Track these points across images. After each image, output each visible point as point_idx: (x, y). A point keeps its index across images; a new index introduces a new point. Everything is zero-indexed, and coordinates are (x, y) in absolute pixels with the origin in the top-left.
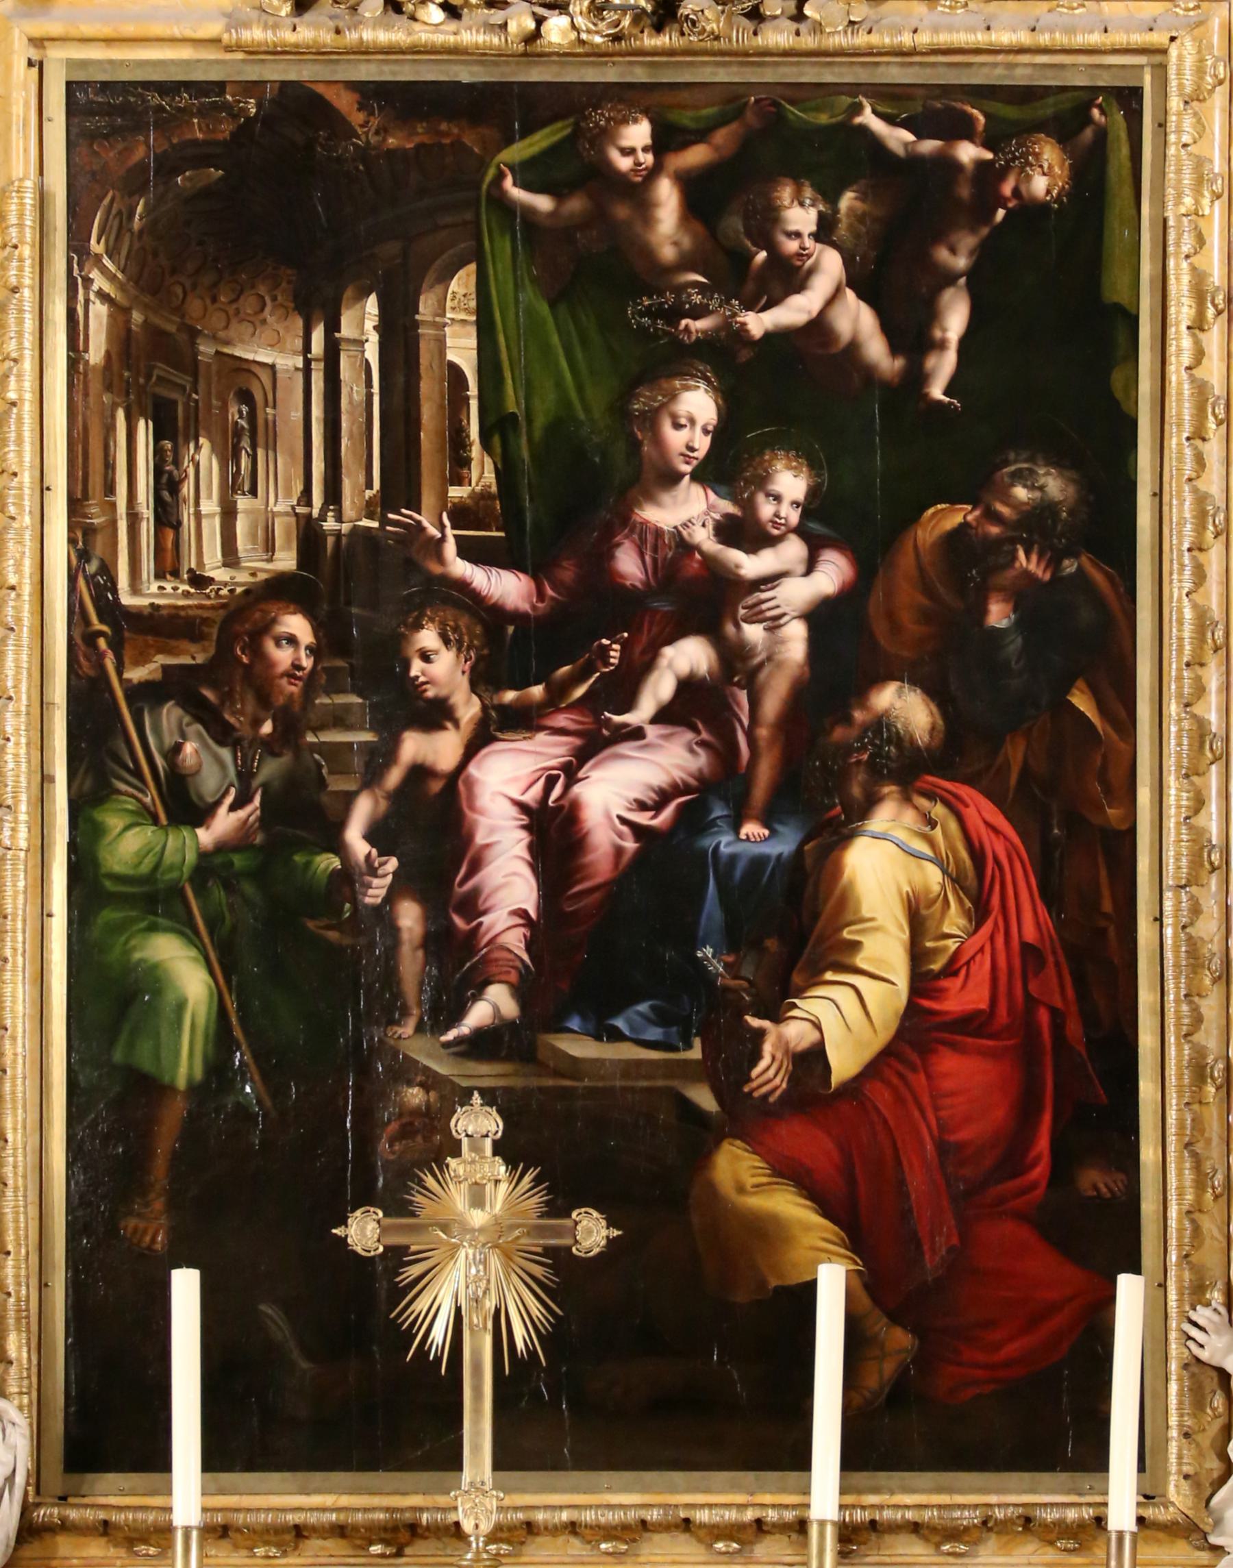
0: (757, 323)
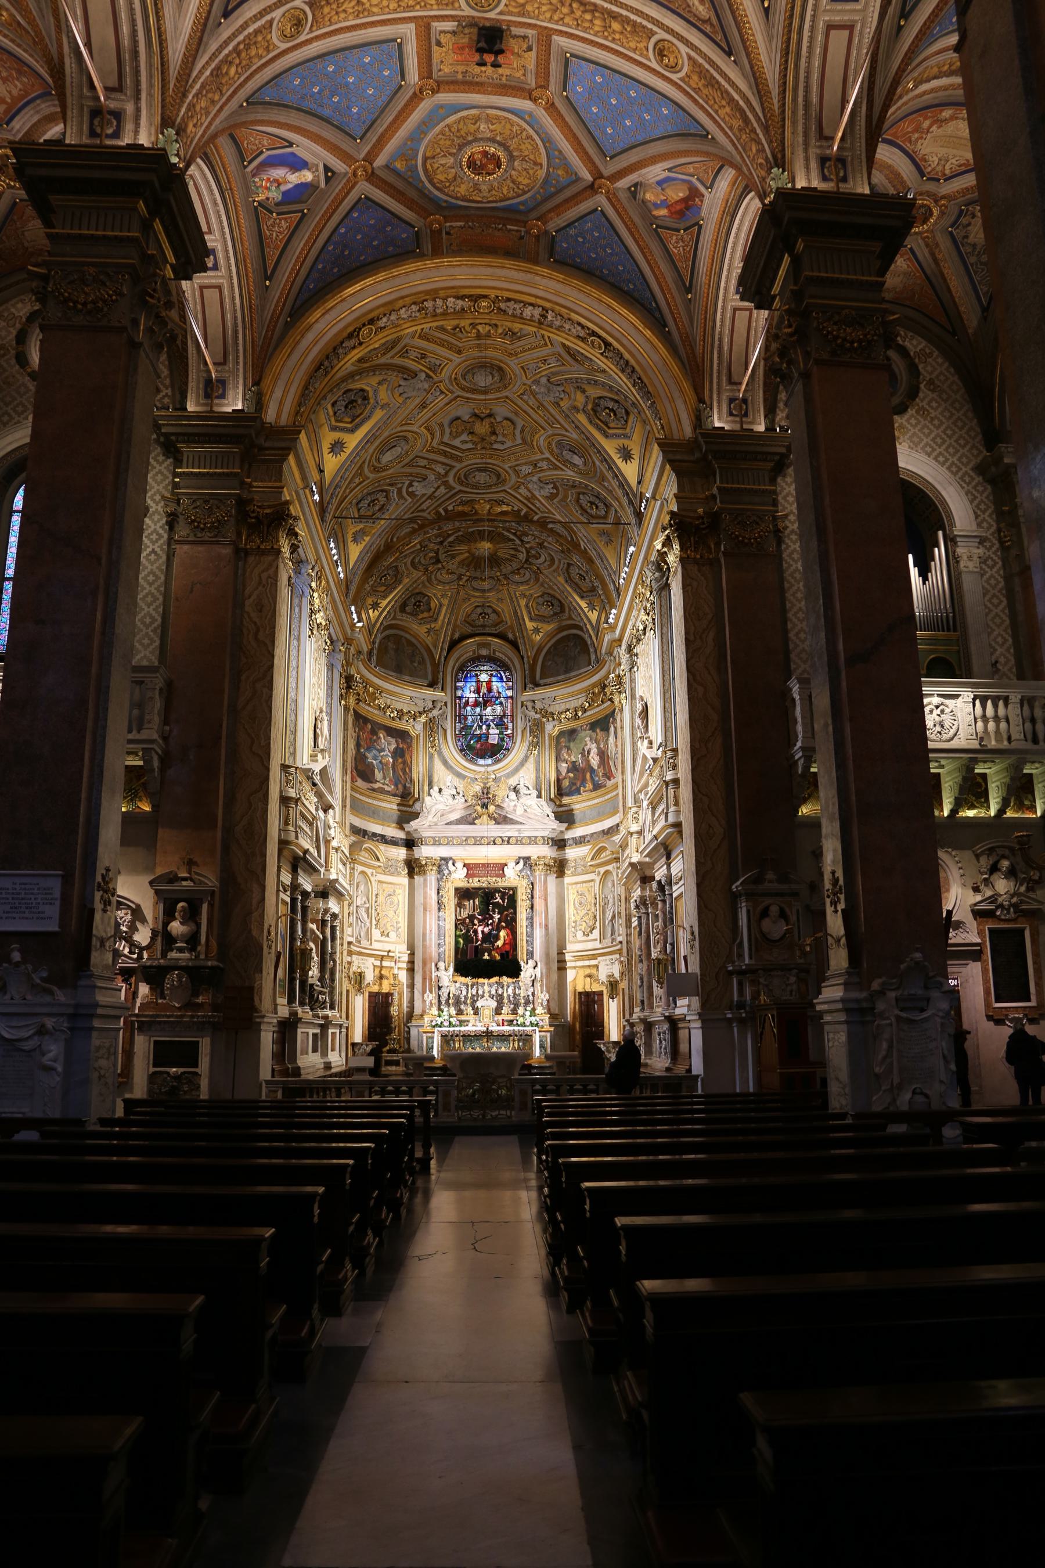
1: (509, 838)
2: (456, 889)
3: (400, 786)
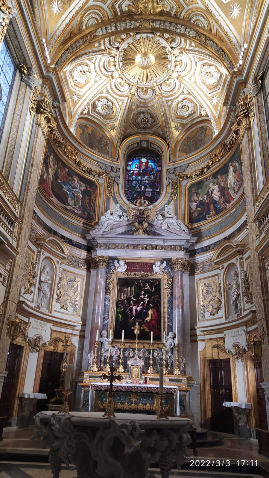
0: (145, 289)
1: (157, 246)
2: (119, 279)
3: (86, 213)
